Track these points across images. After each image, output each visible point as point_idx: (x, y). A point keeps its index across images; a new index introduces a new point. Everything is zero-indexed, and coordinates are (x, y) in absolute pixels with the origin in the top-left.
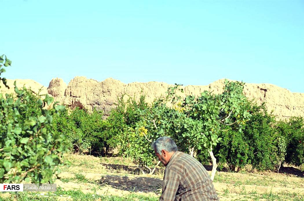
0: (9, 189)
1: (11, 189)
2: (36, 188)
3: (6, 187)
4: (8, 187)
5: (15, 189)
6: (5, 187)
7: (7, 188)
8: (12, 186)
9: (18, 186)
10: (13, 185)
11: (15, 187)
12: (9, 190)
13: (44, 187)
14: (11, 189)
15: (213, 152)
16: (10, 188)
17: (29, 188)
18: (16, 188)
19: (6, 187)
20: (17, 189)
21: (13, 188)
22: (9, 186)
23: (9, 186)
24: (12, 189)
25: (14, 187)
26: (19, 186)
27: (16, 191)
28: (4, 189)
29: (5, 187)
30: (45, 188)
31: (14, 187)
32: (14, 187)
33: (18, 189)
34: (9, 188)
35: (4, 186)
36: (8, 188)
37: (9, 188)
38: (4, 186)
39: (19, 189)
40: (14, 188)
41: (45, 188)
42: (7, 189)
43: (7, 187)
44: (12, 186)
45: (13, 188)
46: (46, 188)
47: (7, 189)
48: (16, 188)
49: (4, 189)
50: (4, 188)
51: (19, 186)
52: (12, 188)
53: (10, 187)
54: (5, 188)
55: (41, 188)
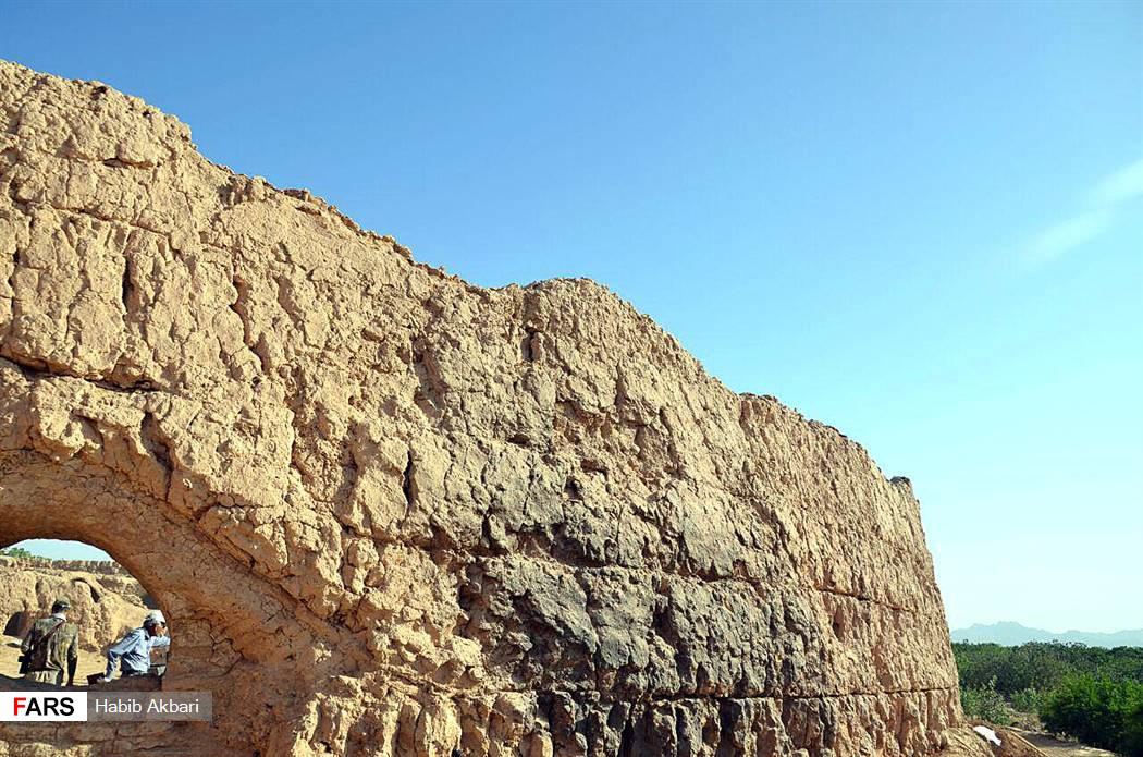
0: (34, 710)
1: (40, 714)
2: (137, 708)
3: (23, 706)
4: (31, 704)
5: (56, 713)
6: (19, 703)
7: (26, 709)
8: (46, 700)
9: (67, 702)
10: (47, 697)
11: (56, 704)
14: (40, 714)
15: (1115, 650)
16: (37, 709)
17: (108, 707)
18: (59, 707)
19: (23, 706)
20: (62, 712)
21: (49, 709)
22: (34, 700)
23: (34, 700)
24: (46, 713)
25: (52, 703)
26: (71, 701)
28: (16, 713)
29: (19, 703)
30: (168, 707)
31: (51, 703)
32: (52, 703)
33: (67, 710)
34: (34, 707)
35: (16, 700)
36: (30, 709)
37: (34, 707)
38: (16, 700)
39: (72, 710)
40: (52, 707)
41: (168, 707)
42: (28, 713)
43: (27, 703)
44: (46, 700)
45: (49, 709)
46: (174, 708)
47: (28, 713)
48: (59, 707)
49: (16, 713)
50: (16, 706)
51: (71, 701)
52: (46, 707)
53: (37, 705)
54: (19, 710)
55: (156, 707)
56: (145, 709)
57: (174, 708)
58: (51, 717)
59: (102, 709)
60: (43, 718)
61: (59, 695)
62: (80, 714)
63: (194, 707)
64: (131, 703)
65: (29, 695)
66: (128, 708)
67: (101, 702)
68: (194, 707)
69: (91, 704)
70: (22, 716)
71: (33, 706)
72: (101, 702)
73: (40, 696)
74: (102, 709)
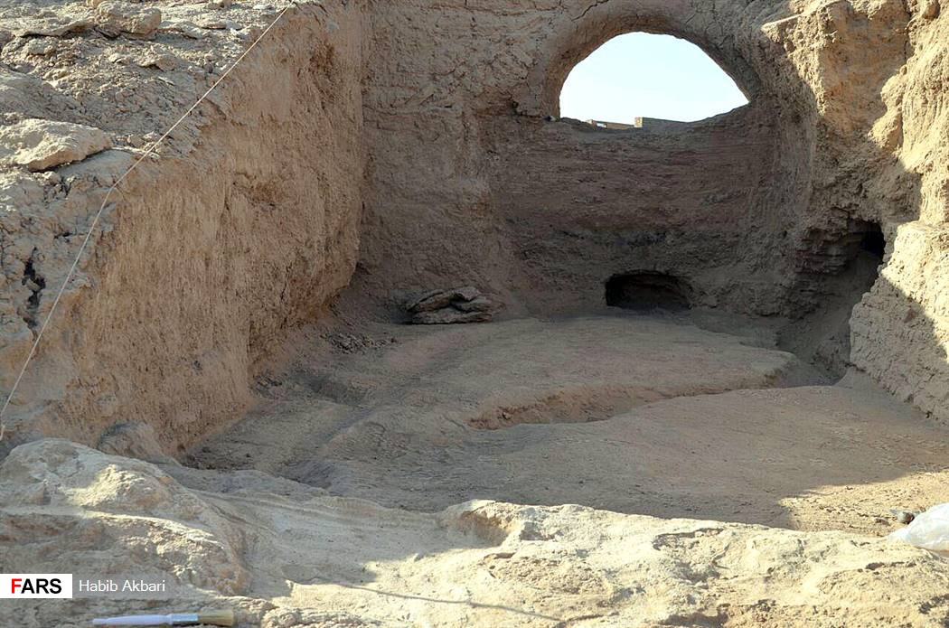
0: (28, 589)
1: (33, 592)
2: (114, 587)
3: (19, 586)
4: (26, 584)
5: (47, 592)
6: (16, 583)
7: (21, 588)
8: (38, 581)
9: (55, 583)
11: (47, 584)
12: (28, 593)
13: (136, 583)
14: (33, 592)
16: (31, 589)
18: (49, 587)
19: (19, 586)
20: (52, 590)
21: (41, 588)
22: (28, 581)
23: (28, 581)
24: (38, 592)
25: (43, 583)
26: (59, 582)
27: (51, 596)
28: (13, 591)
29: (16, 583)
30: (139, 587)
31: (42, 583)
32: (43, 583)
33: (56, 589)
34: (28, 586)
35: (13, 581)
36: (25, 589)
37: (28, 586)
38: (13, 581)
39: (60, 589)
40: (43, 587)
41: (139, 587)
42: (23, 592)
43: (22, 584)
44: (38, 581)
45: (41, 588)
46: (145, 588)
47: (23, 592)
48: (49, 587)
49: (13, 591)
50: (14, 586)
51: (59, 582)
52: (38, 586)
53: (30, 585)
54: (16, 589)
55: (129, 586)
56: (120, 587)
57: (145, 588)
58: (42, 595)
59: (84, 588)
60: (35, 596)
61: (49, 577)
62: (67, 593)
63: (161, 587)
64: (109, 583)
65: (24, 577)
66: (106, 588)
67: (84, 582)
68: (161, 587)
69: (75, 586)
70: (18, 594)
71: (27, 586)
72: (84, 582)
73: (33, 578)
74: (84, 588)
